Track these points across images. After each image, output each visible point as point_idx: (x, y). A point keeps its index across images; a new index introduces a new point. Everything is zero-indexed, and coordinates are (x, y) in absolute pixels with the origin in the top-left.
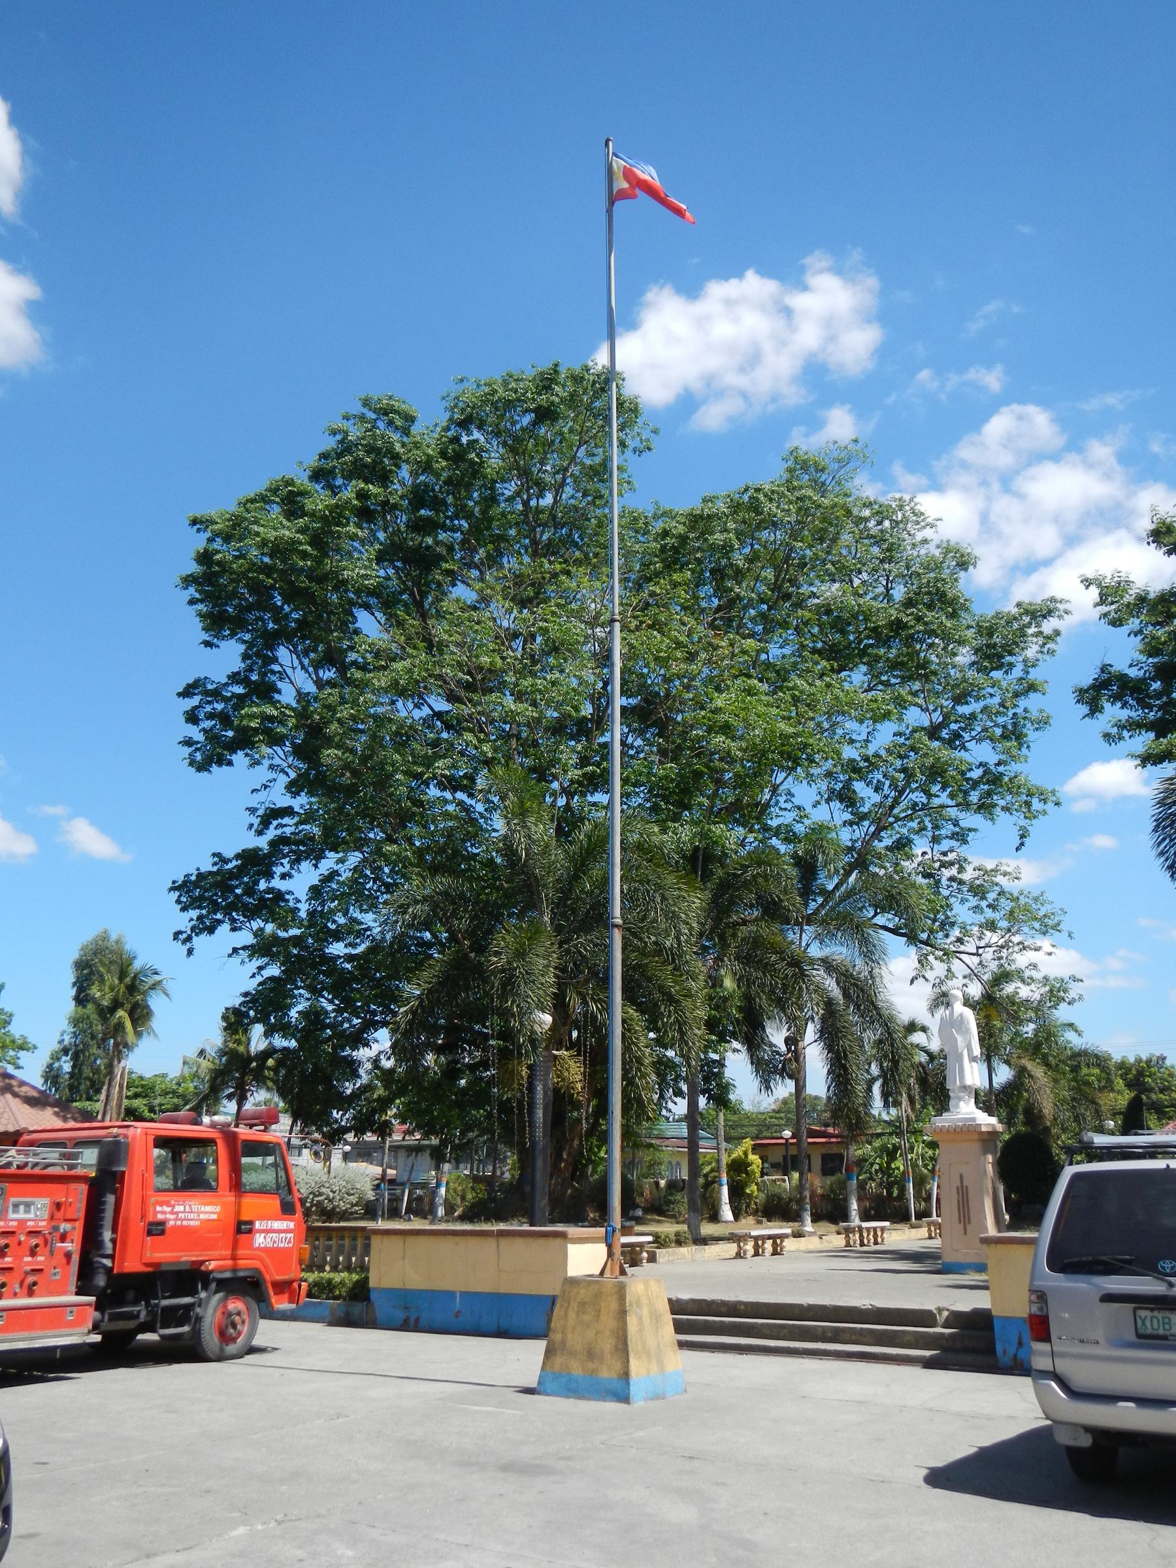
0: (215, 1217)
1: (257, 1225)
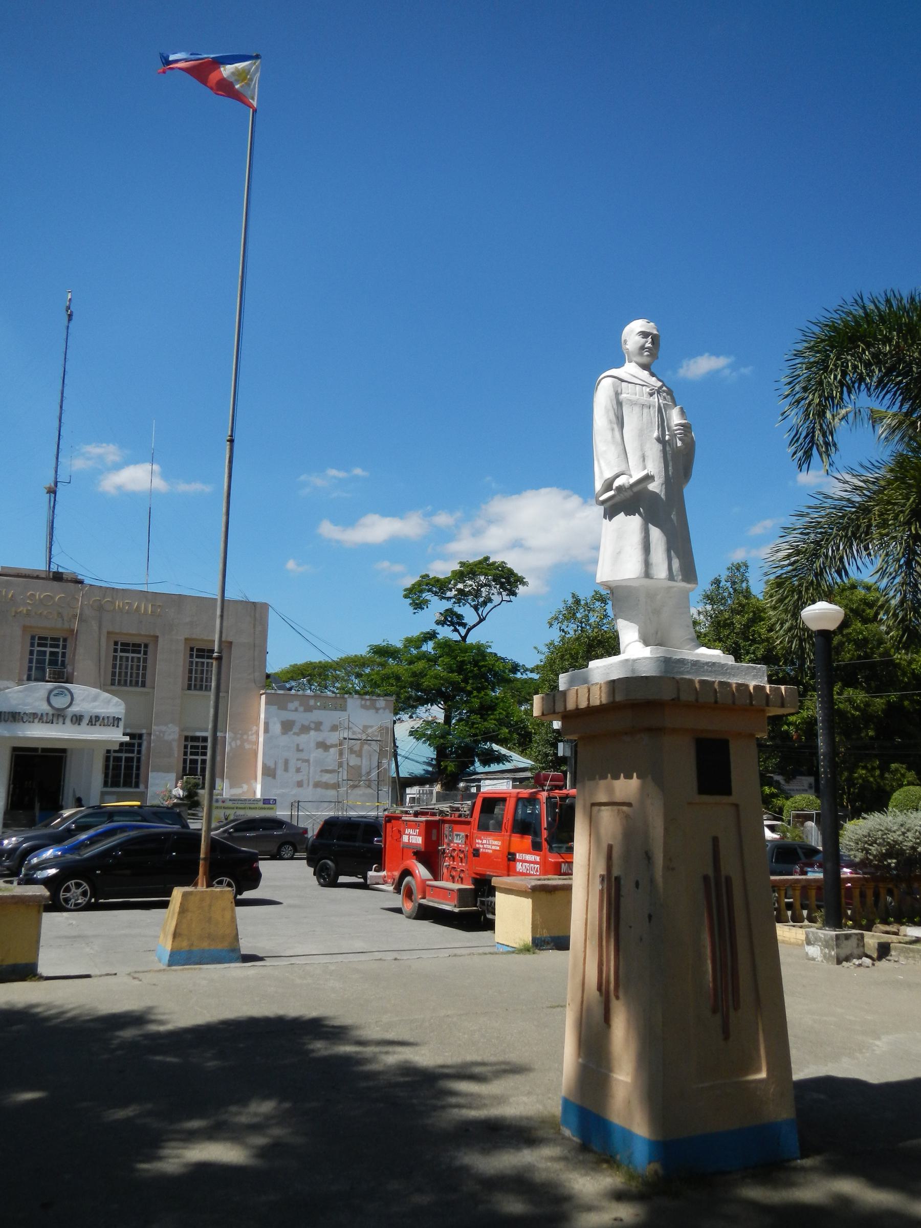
0: (498, 848)
1: (518, 856)
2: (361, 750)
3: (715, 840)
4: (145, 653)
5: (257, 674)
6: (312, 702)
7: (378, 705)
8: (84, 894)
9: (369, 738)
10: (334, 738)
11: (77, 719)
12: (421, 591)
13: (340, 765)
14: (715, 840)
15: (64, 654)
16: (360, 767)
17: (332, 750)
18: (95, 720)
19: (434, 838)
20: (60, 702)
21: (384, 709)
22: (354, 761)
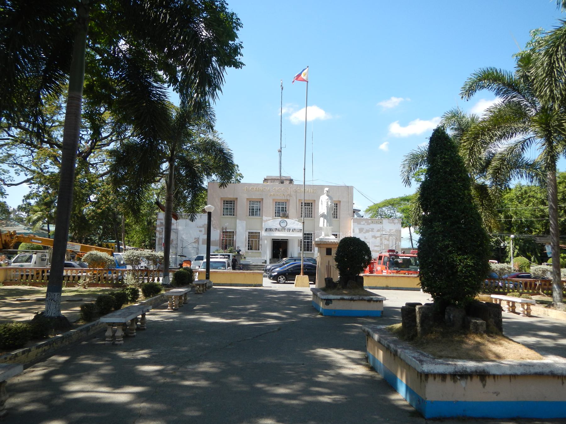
2: (389, 239)
3: (329, 261)
4: (312, 206)
5: (350, 212)
6: (370, 221)
7: (395, 222)
8: (284, 279)
9: (392, 234)
10: (378, 234)
11: (289, 230)
12: (419, 175)
13: (381, 244)
14: (329, 261)
15: (286, 207)
16: (388, 245)
17: (378, 239)
18: (294, 230)
19: (372, 267)
20: (283, 225)
21: (398, 223)
22: (386, 242)
